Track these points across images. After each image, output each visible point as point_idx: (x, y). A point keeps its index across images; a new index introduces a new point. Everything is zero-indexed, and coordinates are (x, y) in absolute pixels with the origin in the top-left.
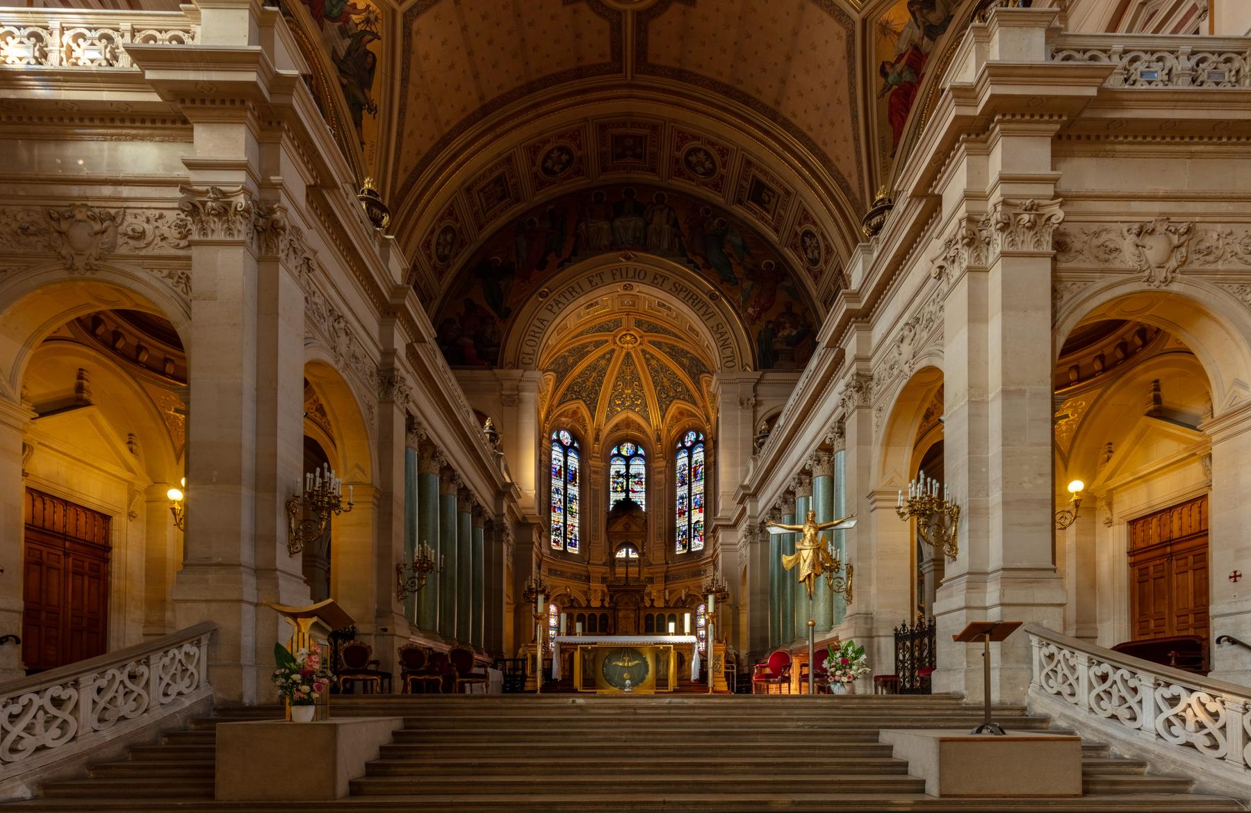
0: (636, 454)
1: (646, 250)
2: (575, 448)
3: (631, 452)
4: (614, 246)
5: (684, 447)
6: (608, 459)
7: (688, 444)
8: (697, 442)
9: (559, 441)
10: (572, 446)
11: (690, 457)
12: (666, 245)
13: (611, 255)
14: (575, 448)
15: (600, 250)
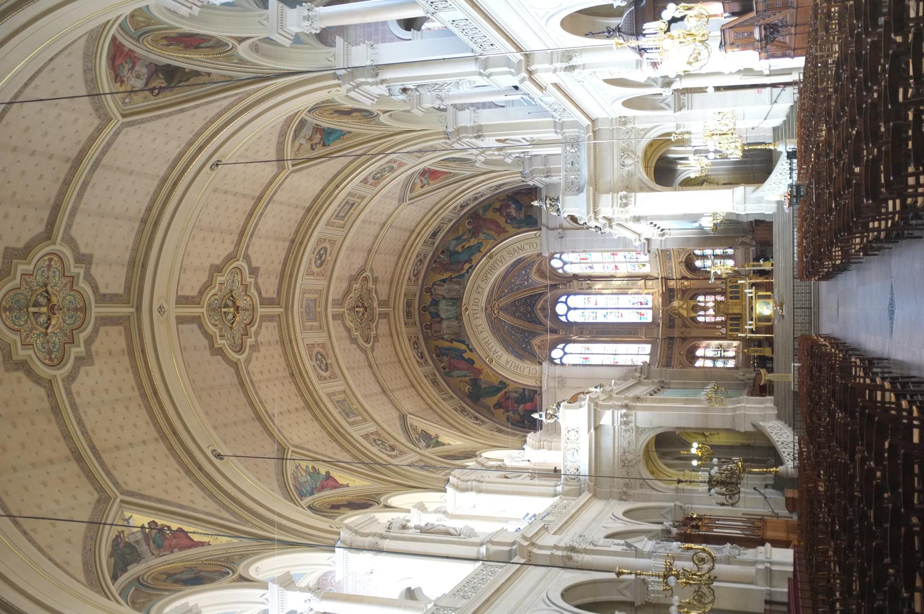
0: (566, 303)
1: (461, 298)
2: (564, 347)
3: (564, 305)
4: (459, 318)
5: (562, 268)
6: (569, 324)
7: (560, 264)
8: (560, 259)
9: (561, 358)
10: (563, 349)
11: (572, 263)
12: (457, 287)
13: (465, 319)
14: (564, 347)
15: (461, 326)
